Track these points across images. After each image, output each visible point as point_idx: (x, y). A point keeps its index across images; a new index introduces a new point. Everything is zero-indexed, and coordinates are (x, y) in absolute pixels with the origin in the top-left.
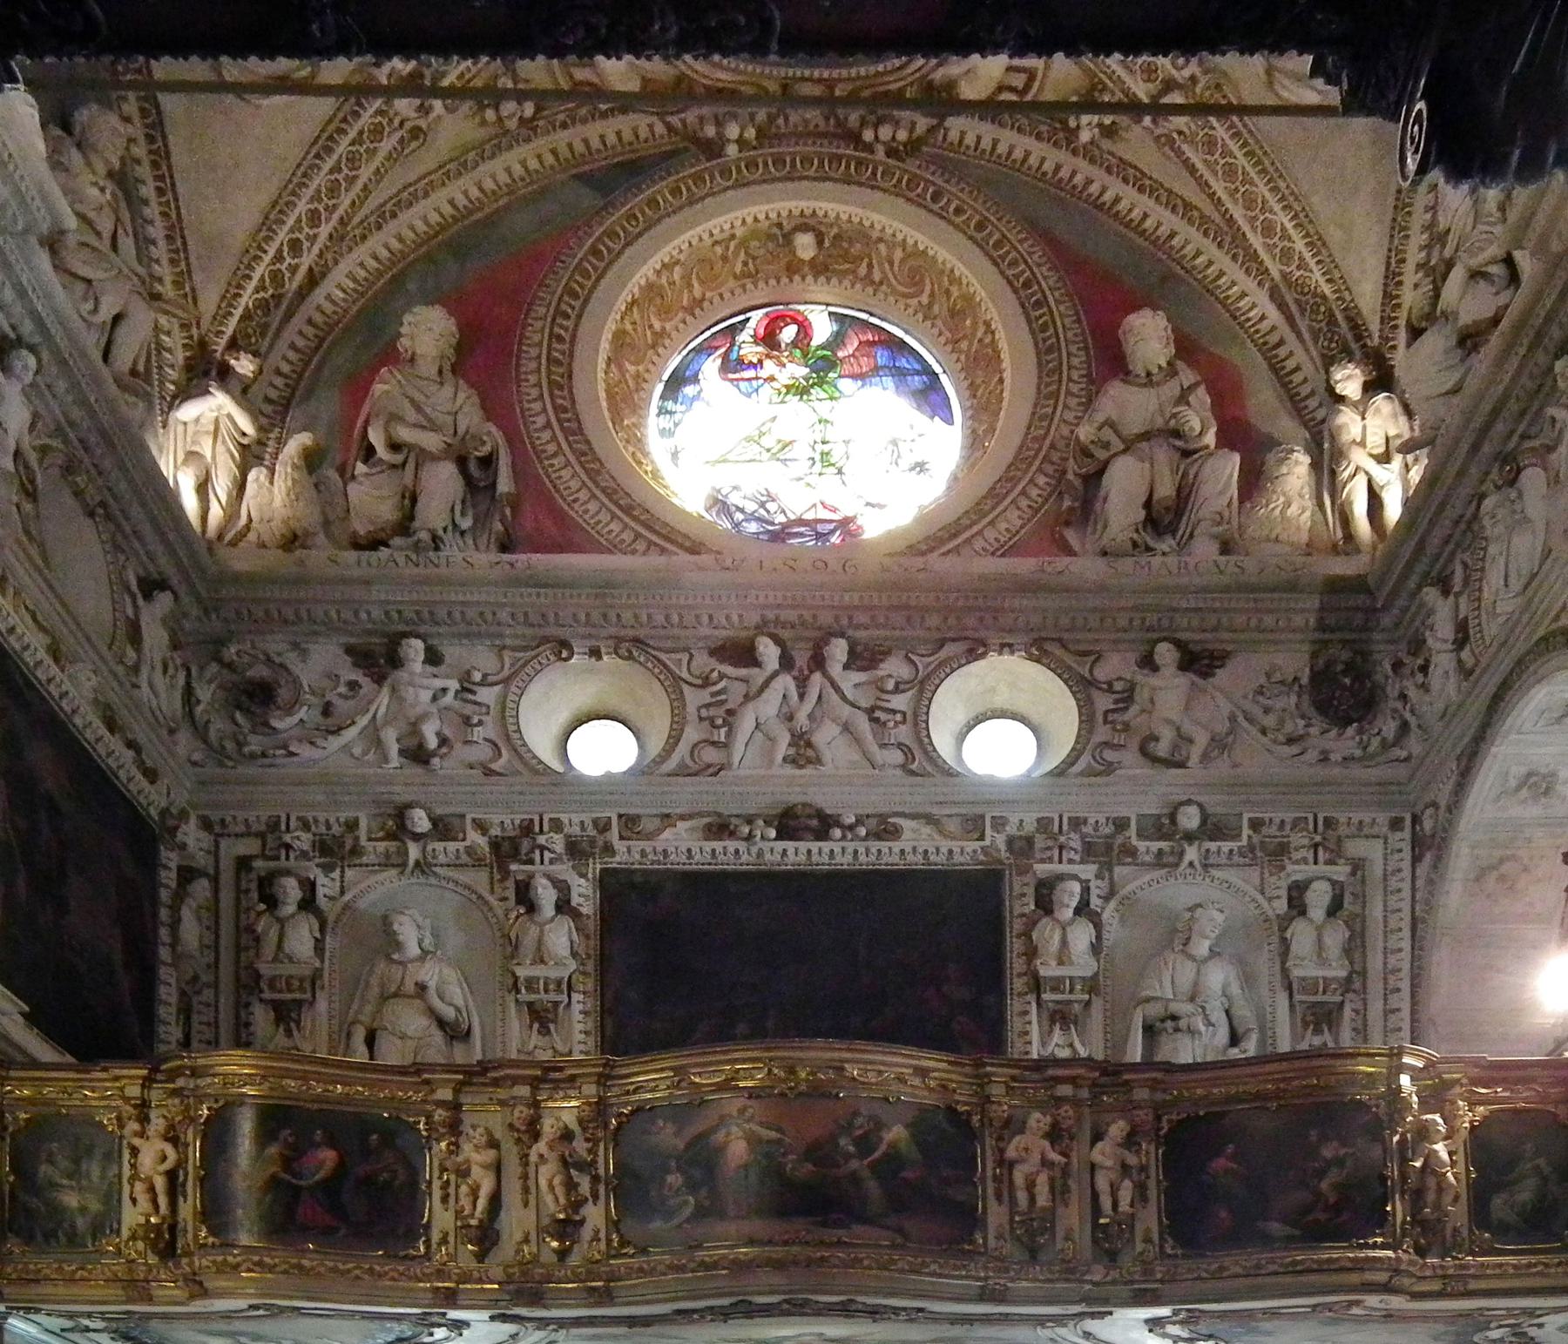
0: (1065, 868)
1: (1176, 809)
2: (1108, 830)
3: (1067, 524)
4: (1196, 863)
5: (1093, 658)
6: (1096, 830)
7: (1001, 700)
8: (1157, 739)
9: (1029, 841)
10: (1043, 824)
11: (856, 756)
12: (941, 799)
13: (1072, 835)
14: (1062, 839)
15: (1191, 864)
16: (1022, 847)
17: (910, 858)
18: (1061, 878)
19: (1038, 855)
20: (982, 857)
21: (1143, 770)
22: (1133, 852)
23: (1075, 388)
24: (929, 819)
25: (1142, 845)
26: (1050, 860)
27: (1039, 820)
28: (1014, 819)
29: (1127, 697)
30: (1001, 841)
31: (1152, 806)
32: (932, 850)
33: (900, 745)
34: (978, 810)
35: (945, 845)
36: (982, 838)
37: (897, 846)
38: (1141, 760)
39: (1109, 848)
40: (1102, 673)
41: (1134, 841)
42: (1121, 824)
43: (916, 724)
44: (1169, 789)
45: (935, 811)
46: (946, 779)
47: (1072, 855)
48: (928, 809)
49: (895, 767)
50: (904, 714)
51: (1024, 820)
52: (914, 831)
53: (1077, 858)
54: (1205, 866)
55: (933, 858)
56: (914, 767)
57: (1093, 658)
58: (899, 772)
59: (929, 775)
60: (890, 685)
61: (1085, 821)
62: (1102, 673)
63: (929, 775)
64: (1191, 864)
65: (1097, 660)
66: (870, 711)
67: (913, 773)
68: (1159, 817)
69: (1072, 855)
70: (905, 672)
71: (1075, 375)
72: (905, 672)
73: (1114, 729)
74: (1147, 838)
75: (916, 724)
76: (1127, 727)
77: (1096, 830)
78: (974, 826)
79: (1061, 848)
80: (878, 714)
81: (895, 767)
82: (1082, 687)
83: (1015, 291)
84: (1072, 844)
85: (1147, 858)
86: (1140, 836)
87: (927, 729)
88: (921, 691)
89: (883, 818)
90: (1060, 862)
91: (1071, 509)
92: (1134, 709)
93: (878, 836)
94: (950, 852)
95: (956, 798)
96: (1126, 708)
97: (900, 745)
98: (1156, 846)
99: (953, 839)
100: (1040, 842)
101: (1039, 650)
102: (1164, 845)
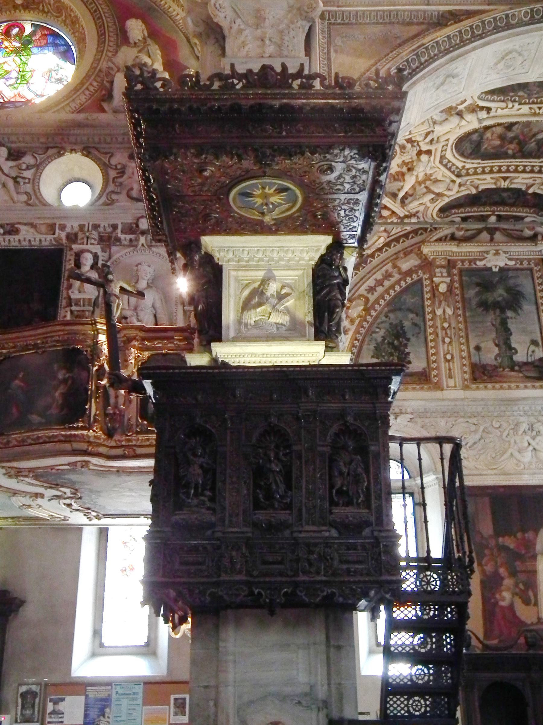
0: (89, 247)
1: (138, 219)
2: (109, 230)
3: (103, 100)
4: (145, 245)
5: (108, 156)
6: (105, 230)
7: (77, 174)
8: (132, 189)
9: (76, 235)
10: (81, 227)
11: (6, 198)
12: (39, 216)
13: (93, 232)
14: (88, 234)
15: (143, 245)
16: (72, 238)
17: (23, 243)
18: (82, 251)
19: (79, 242)
20: (54, 243)
21: (128, 204)
22: (118, 240)
23: (111, 49)
24: (32, 225)
25: (122, 236)
26: (83, 244)
27: (80, 226)
28: (69, 226)
29: (122, 173)
30: (63, 235)
31: (129, 220)
32: (32, 239)
33: (26, 193)
34: (54, 221)
35: (38, 237)
36: (54, 234)
37: (17, 237)
38: (127, 198)
39: (109, 238)
40: (114, 161)
41: (120, 235)
42: (115, 227)
43: (33, 184)
44: (137, 211)
45: (36, 222)
46: (44, 207)
47: (93, 241)
48: (33, 221)
49: (22, 202)
50: (29, 179)
51: (72, 226)
52: (28, 231)
53: (96, 242)
54: (148, 246)
55: (33, 243)
56: (30, 202)
57: (108, 156)
58: (24, 204)
59: (36, 205)
60: (24, 167)
61: (99, 226)
62: (114, 161)
63: (36, 205)
64: (143, 245)
65: (111, 157)
66: (15, 179)
67: (30, 205)
68: (131, 223)
69: (93, 241)
70: (31, 161)
71: (111, 44)
72: (31, 161)
73: (116, 186)
74: (126, 233)
75: (33, 184)
76: (121, 184)
77: (105, 230)
78: (52, 228)
79: (88, 238)
80: (19, 179)
81: (22, 202)
82: (105, 167)
83: (92, 14)
84: (93, 236)
85: (126, 243)
86: (122, 232)
87: (39, 186)
88: (38, 169)
89: (12, 225)
90: (87, 244)
91: (104, 95)
92: (125, 176)
93: (9, 233)
94: (40, 240)
95: (46, 216)
96: (122, 176)
97: (26, 193)
98: (128, 237)
99: (41, 234)
100: (80, 235)
101: (87, 152)
102: (132, 236)
